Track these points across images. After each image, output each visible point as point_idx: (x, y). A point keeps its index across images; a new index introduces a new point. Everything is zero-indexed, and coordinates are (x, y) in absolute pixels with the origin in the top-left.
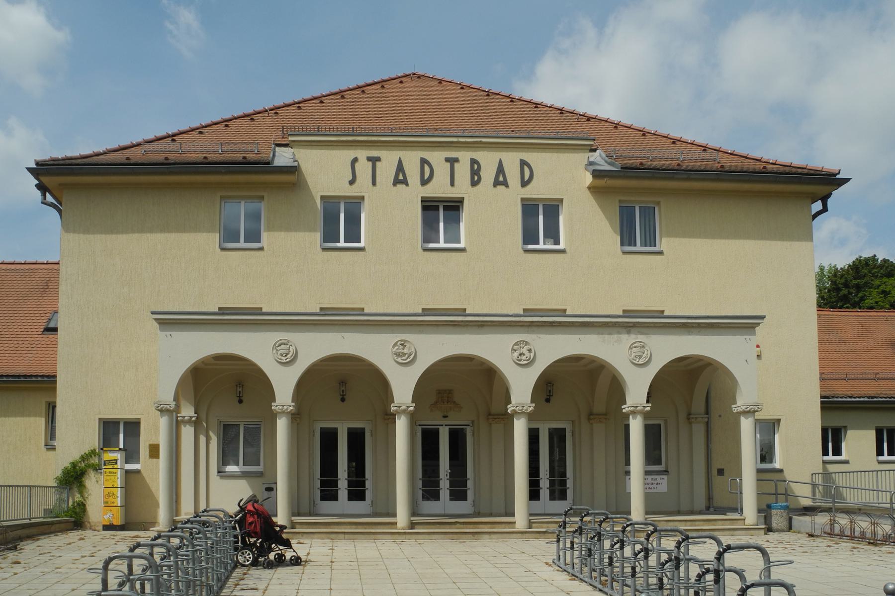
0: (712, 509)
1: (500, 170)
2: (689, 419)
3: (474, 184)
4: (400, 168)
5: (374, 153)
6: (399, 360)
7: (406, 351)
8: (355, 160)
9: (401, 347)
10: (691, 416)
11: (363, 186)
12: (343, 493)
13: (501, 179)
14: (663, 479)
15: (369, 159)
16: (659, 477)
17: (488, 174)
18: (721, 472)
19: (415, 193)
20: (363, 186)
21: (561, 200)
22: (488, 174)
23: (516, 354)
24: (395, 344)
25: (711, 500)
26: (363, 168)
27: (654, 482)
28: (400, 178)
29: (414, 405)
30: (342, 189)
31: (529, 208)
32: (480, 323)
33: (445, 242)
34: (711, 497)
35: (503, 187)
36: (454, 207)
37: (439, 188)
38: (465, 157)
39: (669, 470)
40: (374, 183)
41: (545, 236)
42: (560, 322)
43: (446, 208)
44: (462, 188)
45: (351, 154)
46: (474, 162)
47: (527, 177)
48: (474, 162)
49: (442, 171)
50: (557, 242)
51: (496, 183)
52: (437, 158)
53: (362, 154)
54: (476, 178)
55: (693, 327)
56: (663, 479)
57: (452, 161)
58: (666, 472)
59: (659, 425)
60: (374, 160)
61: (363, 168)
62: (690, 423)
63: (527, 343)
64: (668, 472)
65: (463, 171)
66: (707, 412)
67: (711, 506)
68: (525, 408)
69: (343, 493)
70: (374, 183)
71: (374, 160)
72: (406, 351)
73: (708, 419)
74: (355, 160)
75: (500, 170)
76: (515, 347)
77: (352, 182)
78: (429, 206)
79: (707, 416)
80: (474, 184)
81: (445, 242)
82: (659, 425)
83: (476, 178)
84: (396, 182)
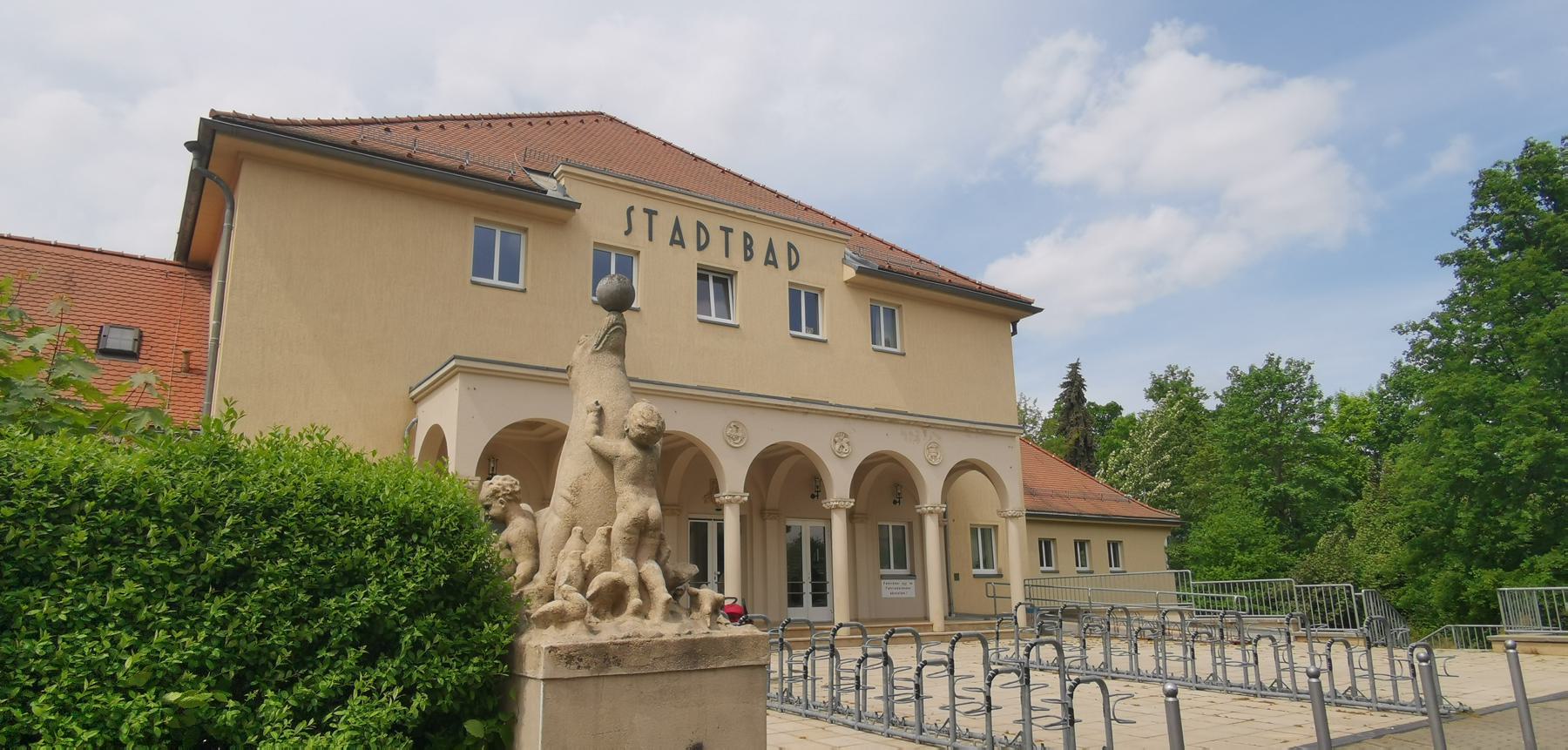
1: (771, 249)
3: (747, 259)
4: (677, 228)
5: (652, 205)
6: (732, 444)
7: (740, 434)
8: (631, 209)
9: (735, 429)
11: (639, 239)
12: (807, 598)
13: (771, 259)
15: (646, 211)
17: (760, 250)
18: (957, 577)
19: (690, 259)
20: (639, 239)
21: (822, 291)
22: (760, 250)
23: (837, 446)
24: (729, 426)
26: (640, 219)
28: (677, 240)
29: (748, 494)
30: (620, 240)
31: (794, 295)
32: (806, 411)
33: (717, 316)
35: (773, 267)
36: (724, 280)
37: (714, 257)
38: (739, 228)
40: (651, 239)
41: (807, 325)
42: (873, 417)
43: (715, 280)
44: (735, 262)
45: (627, 200)
46: (746, 236)
47: (793, 262)
48: (746, 236)
49: (717, 238)
50: (816, 332)
51: (767, 262)
52: (713, 223)
53: (640, 203)
54: (749, 254)
55: (972, 432)
57: (727, 231)
58: (912, 576)
59: (903, 527)
60: (651, 213)
61: (640, 219)
63: (846, 436)
65: (737, 242)
68: (847, 503)
69: (807, 598)
70: (651, 239)
71: (651, 213)
72: (740, 434)
74: (631, 209)
75: (771, 249)
76: (837, 439)
77: (627, 233)
78: (703, 274)
80: (747, 259)
81: (717, 316)
82: (903, 527)
83: (749, 254)
84: (673, 242)
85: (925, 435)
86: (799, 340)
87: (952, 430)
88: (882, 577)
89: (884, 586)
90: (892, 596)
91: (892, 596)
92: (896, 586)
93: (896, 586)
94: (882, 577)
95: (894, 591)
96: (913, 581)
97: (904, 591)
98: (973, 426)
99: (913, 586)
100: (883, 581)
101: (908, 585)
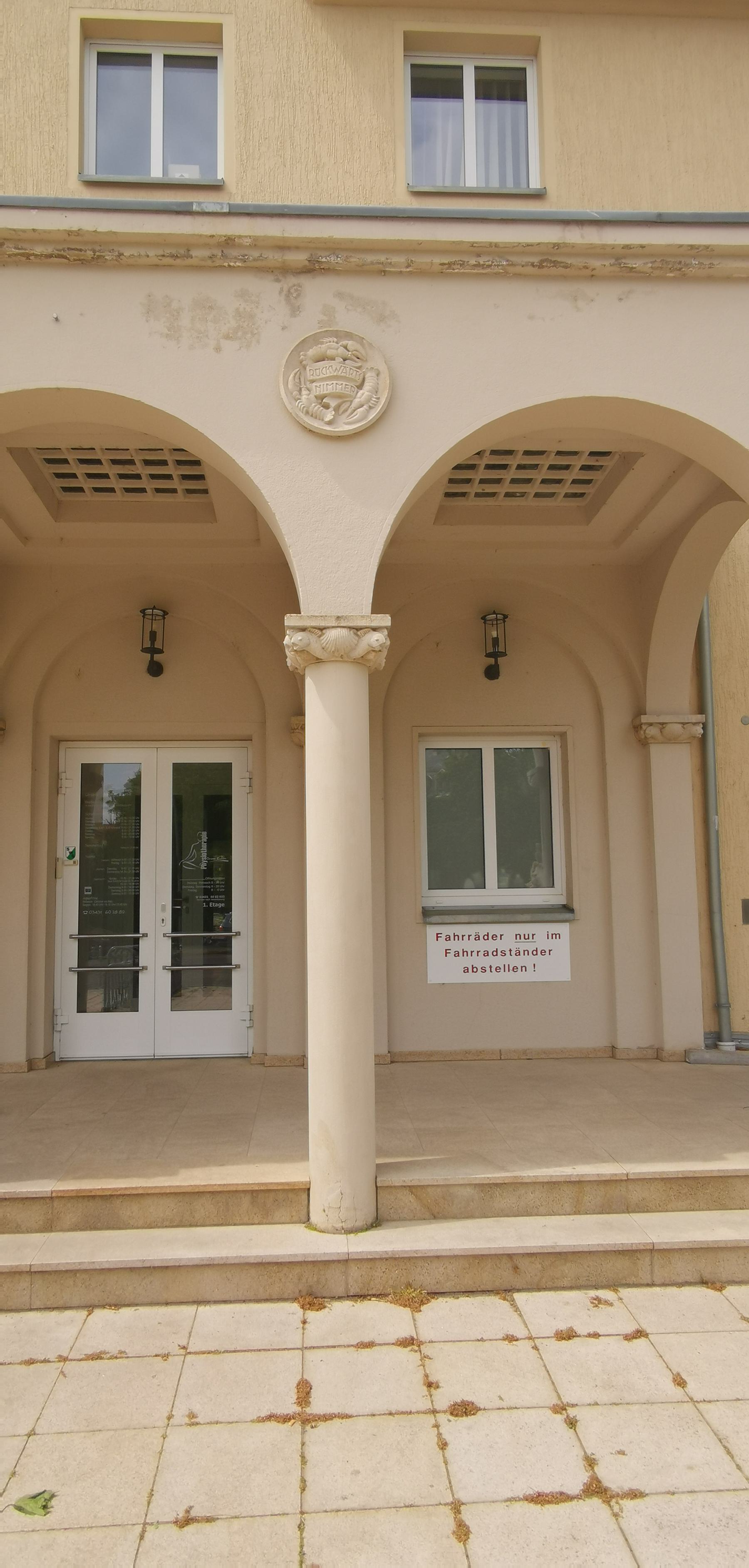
0: (728, 1046)
2: (637, 727)
10: (644, 719)
14: (557, 936)
16: (540, 930)
25: (724, 1011)
27: (523, 946)
34: (723, 1000)
39: (576, 906)
56: (557, 936)
62: (644, 743)
64: (571, 910)
66: (701, 709)
67: (725, 1035)
73: (704, 728)
79: (700, 718)
85: (295, 311)
86: (130, 208)
87: (445, 272)
88: (428, 914)
89: (435, 948)
90: (471, 978)
91: (471, 978)
92: (490, 945)
93: (490, 945)
94: (428, 914)
95: (480, 961)
96: (564, 929)
97: (527, 960)
98: (574, 236)
99: (562, 948)
100: (432, 931)
101: (541, 942)
